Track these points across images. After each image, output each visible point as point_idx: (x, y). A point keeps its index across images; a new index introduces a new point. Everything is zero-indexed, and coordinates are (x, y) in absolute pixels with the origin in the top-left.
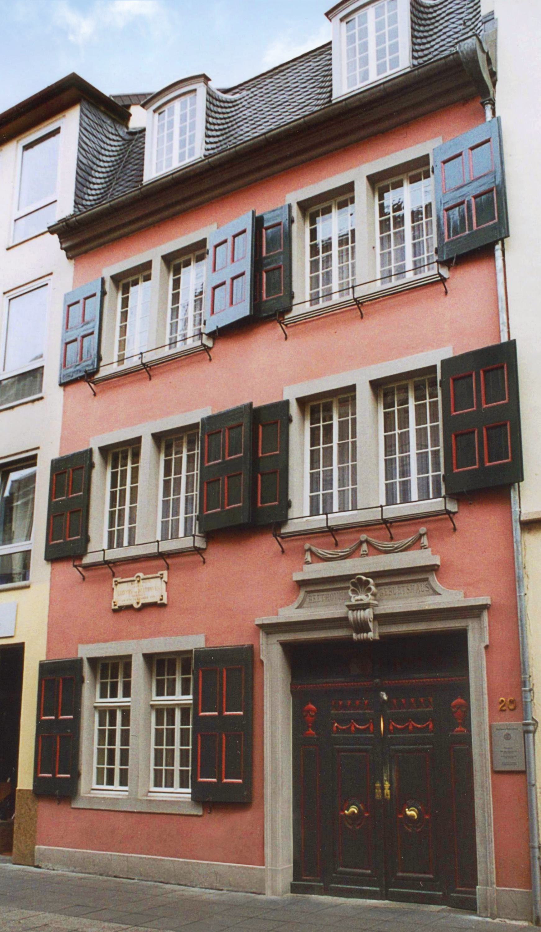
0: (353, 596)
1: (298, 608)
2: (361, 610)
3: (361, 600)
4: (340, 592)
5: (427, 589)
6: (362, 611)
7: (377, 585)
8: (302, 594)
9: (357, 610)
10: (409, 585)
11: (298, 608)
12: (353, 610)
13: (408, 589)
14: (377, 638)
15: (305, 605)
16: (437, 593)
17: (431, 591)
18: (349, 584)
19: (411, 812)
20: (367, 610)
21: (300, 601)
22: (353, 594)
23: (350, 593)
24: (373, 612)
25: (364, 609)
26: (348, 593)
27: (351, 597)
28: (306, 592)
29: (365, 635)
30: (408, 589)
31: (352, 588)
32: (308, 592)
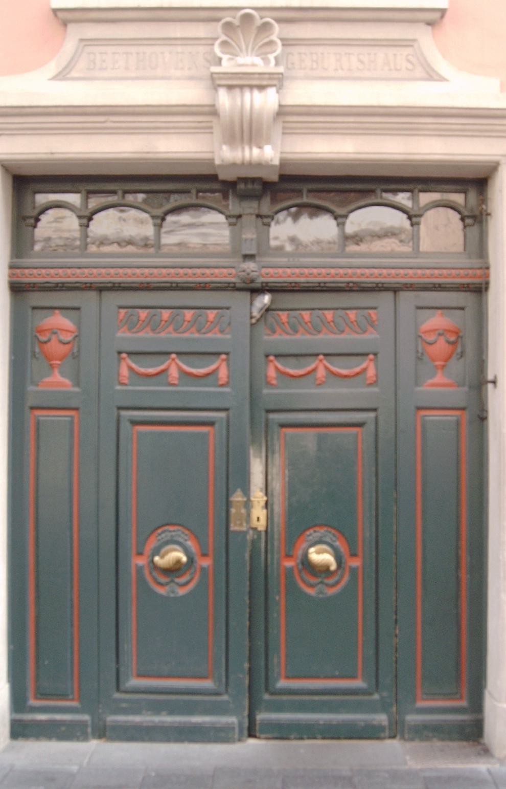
0: (225, 58)
1: (54, 78)
2: (251, 87)
3: (253, 65)
4: (179, 49)
5: (410, 66)
6: (256, 93)
7: (286, 42)
8: (70, 45)
9: (241, 87)
10: (365, 50)
11: (54, 78)
12: (230, 87)
13: (362, 62)
14: (276, 162)
15: (74, 74)
16: (432, 75)
17: (419, 72)
18: (217, 29)
19: (321, 556)
20: (272, 92)
21: (64, 63)
22: (223, 53)
23: (217, 50)
24: (279, 102)
25: (262, 88)
26: (213, 50)
27: (220, 59)
28: (82, 40)
29: (256, 151)
30: (362, 62)
31: (223, 38)
32: (85, 45)
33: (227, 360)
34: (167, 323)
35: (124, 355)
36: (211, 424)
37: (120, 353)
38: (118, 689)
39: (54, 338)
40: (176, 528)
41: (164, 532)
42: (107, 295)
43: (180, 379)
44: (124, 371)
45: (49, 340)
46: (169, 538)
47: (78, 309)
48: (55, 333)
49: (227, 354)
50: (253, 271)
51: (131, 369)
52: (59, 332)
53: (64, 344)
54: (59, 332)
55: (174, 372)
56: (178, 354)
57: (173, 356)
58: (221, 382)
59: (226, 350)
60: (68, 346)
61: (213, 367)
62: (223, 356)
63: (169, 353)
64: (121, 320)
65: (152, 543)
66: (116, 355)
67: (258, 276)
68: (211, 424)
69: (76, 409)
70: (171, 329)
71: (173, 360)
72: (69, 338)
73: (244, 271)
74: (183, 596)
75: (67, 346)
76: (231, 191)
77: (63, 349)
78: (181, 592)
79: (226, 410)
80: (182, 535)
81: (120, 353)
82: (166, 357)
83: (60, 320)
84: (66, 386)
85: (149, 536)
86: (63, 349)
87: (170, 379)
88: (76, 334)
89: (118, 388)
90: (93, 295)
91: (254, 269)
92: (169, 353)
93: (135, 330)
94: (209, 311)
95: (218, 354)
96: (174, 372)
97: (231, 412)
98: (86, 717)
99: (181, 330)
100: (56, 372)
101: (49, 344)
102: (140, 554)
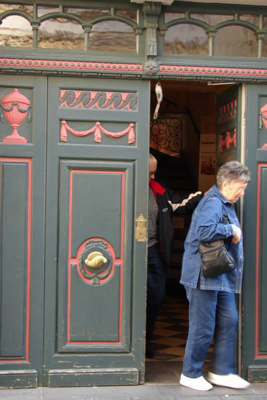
33: (134, 127)
34: (110, 101)
35: (64, 122)
36: (123, 170)
37: (61, 120)
38: (56, 352)
39: (15, 108)
40: (98, 240)
41: (90, 243)
42: (51, 79)
43: (101, 139)
44: (64, 132)
45: (12, 110)
46: (94, 247)
47: (31, 88)
48: (16, 105)
49: (134, 123)
50: (154, 67)
51: (68, 131)
52: (19, 104)
53: (23, 112)
54: (19, 104)
55: (98, 135)
56: (100, 122)
57: (98, 123)
58: (130, 142)
59: (133, 121)
60: (24, 114)
61: (125, 132)
62: (132, 125)
63: (95, 121)
64: (62, 98)
65: (83, 250)
66: (59, 121)
67: (157, 71)
68: (123, 170)
69: (30, 158)
70: (97, 104)
71: (98, 126)
72: (24, 107)
73: (149, 67)
74: (104, 286)
75: (24, 114)
76: (138, 10)
77: (22, 116)
78: (103, 282)
79: (134, 161)
80: (103, 245)
81: (61, 120)
82: (93, 124)
83: (17, 96)
84: (23, 142)
85: (80, 245)
86: (22, 116)
87: (95, 139)
88: (30, 106)
89: (59, 144)
90: (43, 80)
91: (155, 66)
92: (95, 121)
93: (71, 105)
94: (122, 94)
95: (129, 123)
96: (98, 135)
97: (136, 162)
98: (35, 371)
99: (103, 106)
100: (16, 132)
101: (11, 112)
102: (74, 258)
